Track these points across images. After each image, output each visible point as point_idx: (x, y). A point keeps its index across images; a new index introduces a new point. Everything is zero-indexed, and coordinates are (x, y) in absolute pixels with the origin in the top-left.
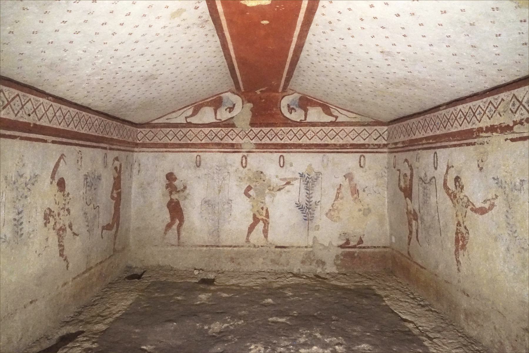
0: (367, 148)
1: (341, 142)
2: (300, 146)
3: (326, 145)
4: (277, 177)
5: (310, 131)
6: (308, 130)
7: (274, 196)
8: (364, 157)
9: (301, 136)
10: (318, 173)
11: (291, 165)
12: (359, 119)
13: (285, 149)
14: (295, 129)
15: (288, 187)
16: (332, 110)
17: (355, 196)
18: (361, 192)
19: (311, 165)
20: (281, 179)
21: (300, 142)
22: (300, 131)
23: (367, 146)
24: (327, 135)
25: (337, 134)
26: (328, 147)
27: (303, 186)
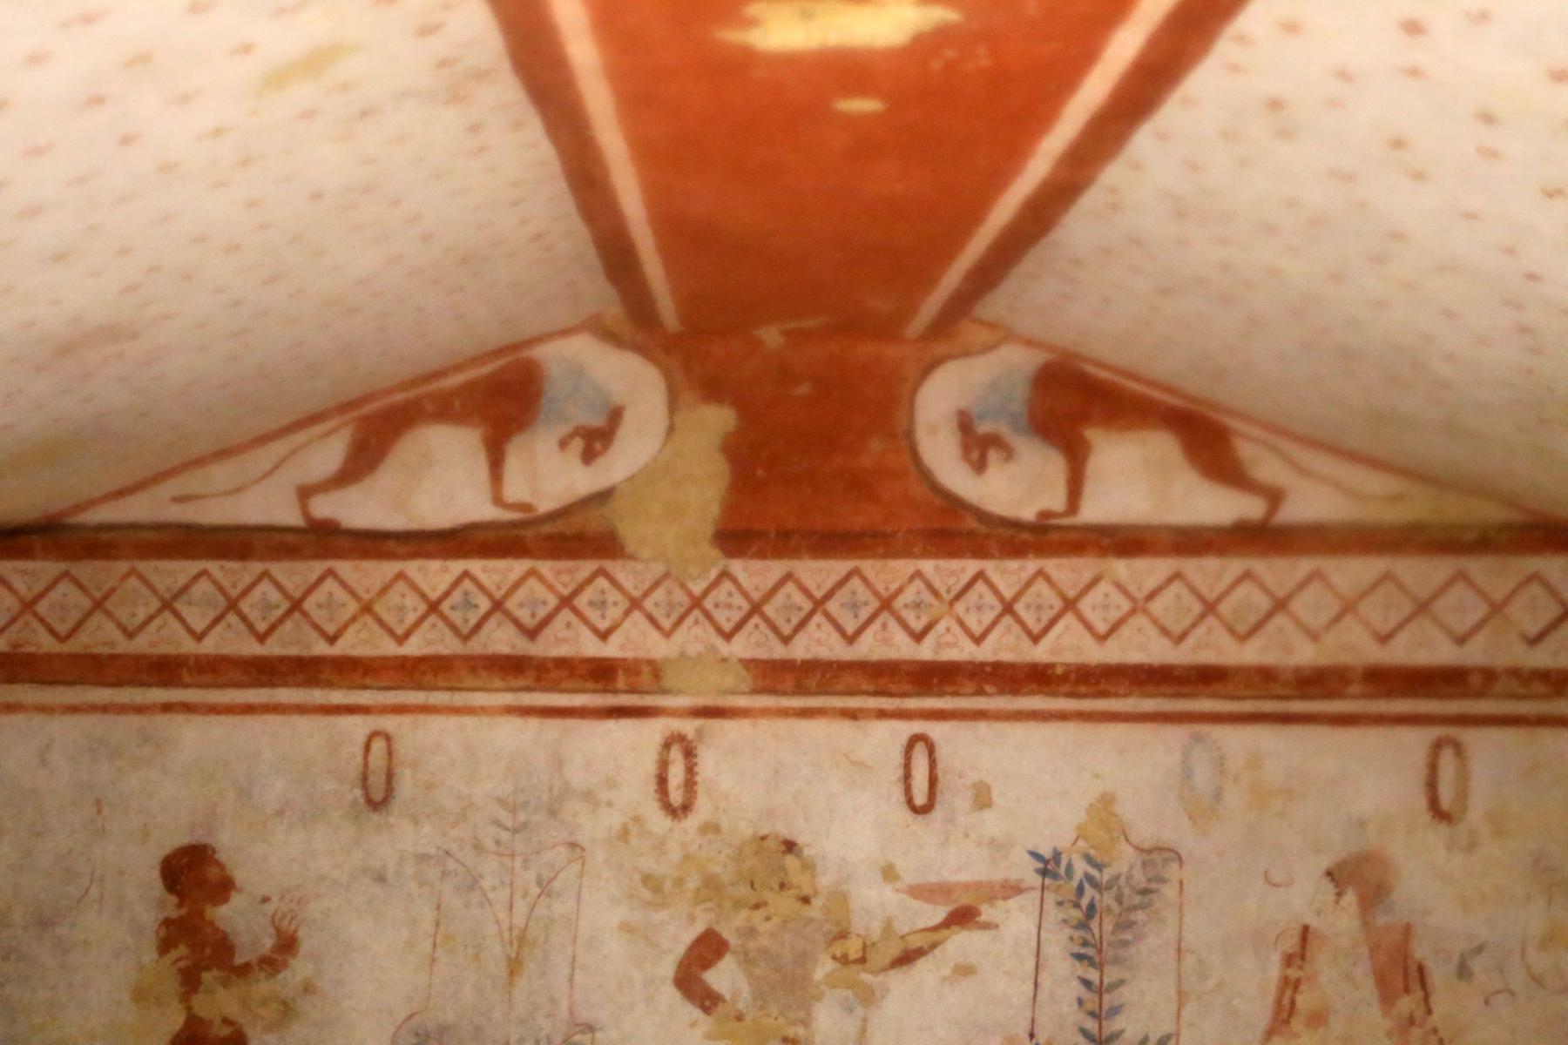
0: (1480, 694)
1: (1305, 654)
2: (1039, 677)
3: (1208, 677)
4: (889, 874)
5: (1104, 587)
6: (1087, 576)
7: (869, 997)
8: (1458, 748)
9: (1046, 616)
10: (1159, 855)
11: (982, 798)
12: (1418, 507)
13: (941, 694)
14: (1008, 573)
15: (961, 942)
16: (1246, 451)
17: (1406, 1004)
18: (1440, 976)
19: (1107, 800)
20: (922, 892)
21: (1040, 654)
22: (1041, 586)
23: (1475, 681)
24: (1210, 608)
25: (1280, 605)
26: (1217, 687)
27: (1058, 944)
